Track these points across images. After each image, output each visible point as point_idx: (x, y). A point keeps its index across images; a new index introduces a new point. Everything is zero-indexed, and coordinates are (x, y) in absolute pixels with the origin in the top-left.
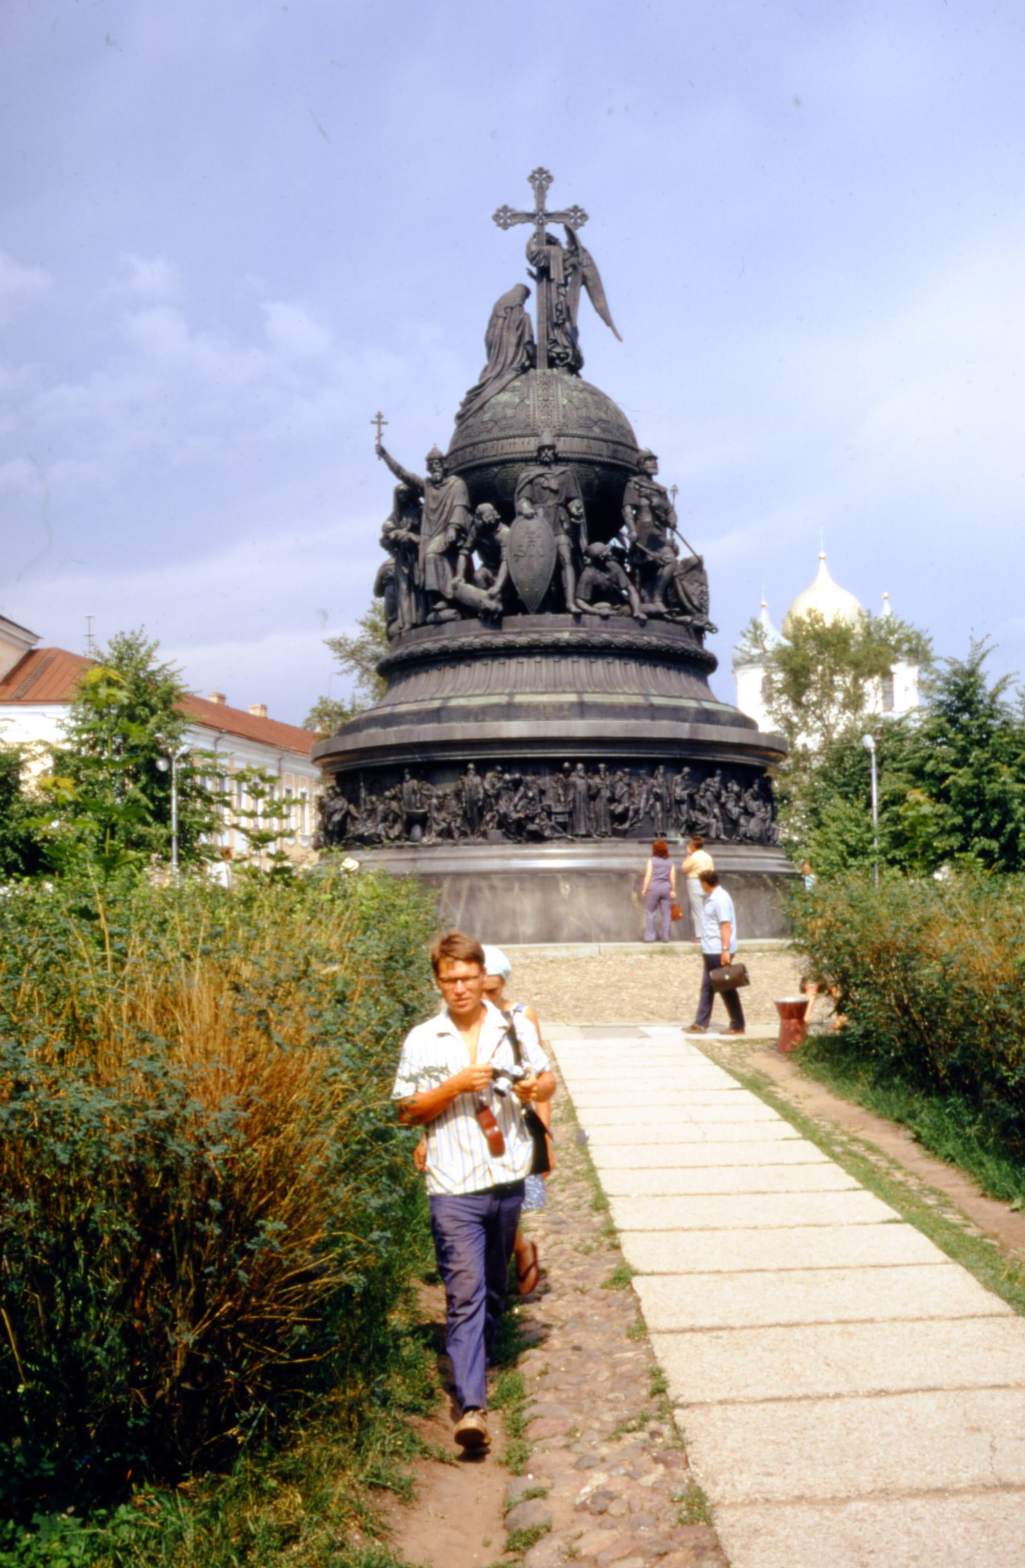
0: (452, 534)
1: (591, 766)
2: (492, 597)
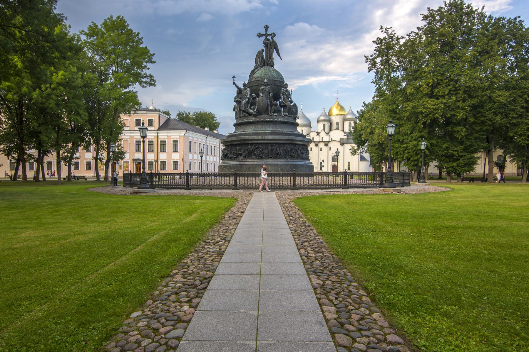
0: (247, 100)
2: (254, 112)
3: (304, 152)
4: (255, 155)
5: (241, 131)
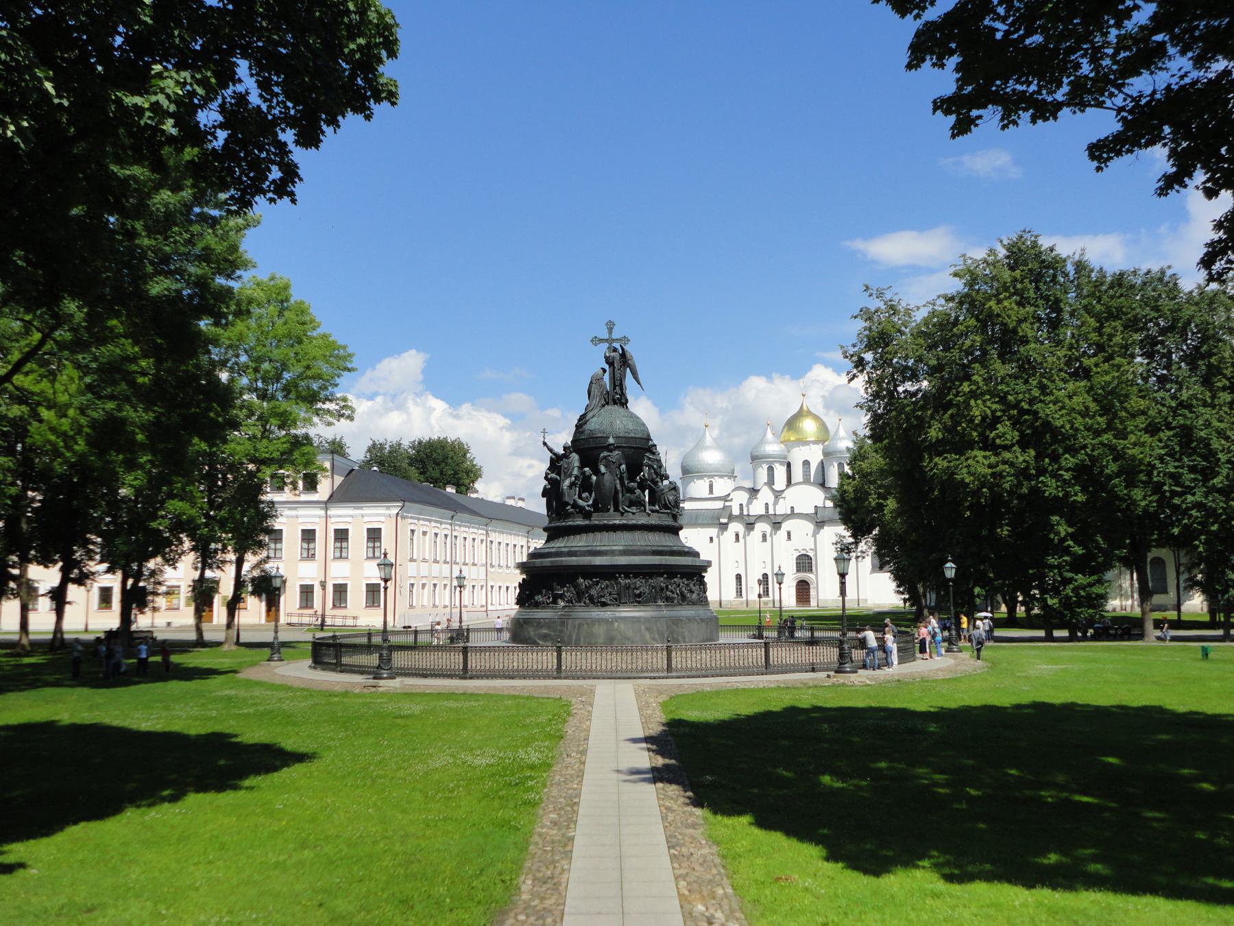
0: (573, 479)
1: (627, 577)
3: (694, 588)
4: (591, 599)
5: (560, 544)
